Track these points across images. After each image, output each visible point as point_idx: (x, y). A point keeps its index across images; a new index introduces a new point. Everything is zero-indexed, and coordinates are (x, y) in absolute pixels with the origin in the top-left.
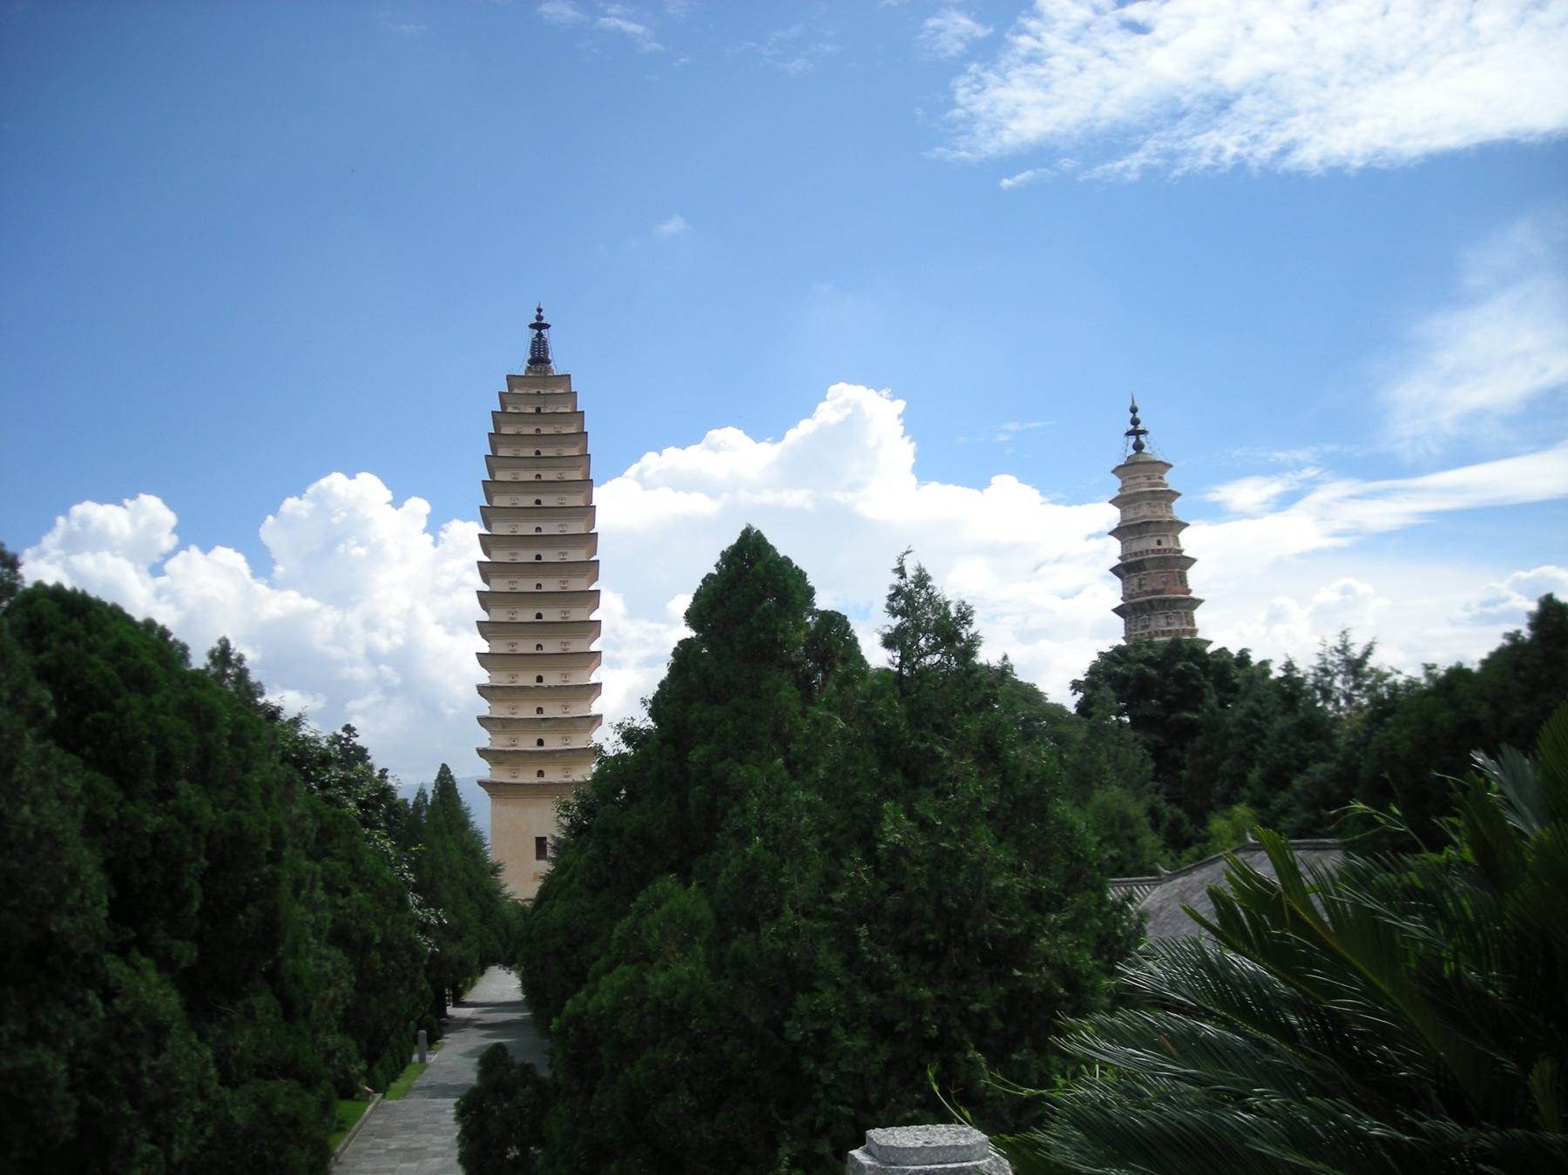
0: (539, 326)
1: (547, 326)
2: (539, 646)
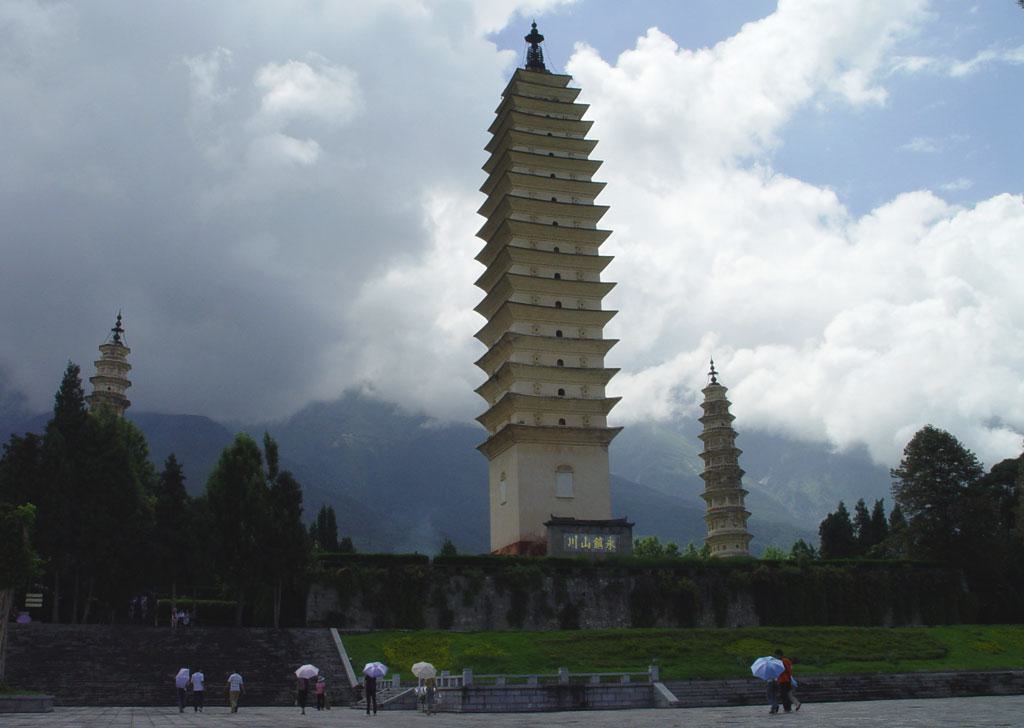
1: (541, 38)
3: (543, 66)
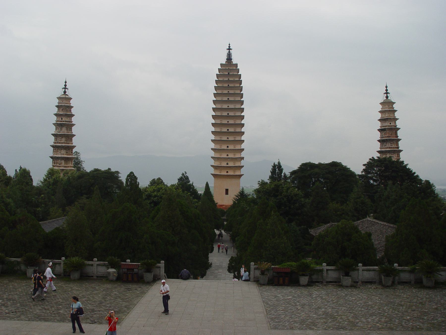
0: (229, 49)
2: (228, 138)
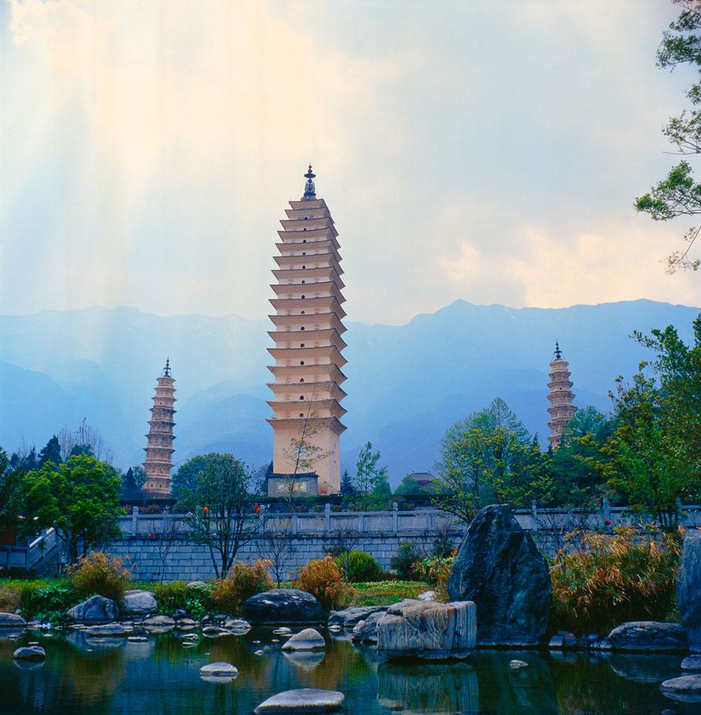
0: (310, 175)
1: (314, 176)
3: (315, 195)
